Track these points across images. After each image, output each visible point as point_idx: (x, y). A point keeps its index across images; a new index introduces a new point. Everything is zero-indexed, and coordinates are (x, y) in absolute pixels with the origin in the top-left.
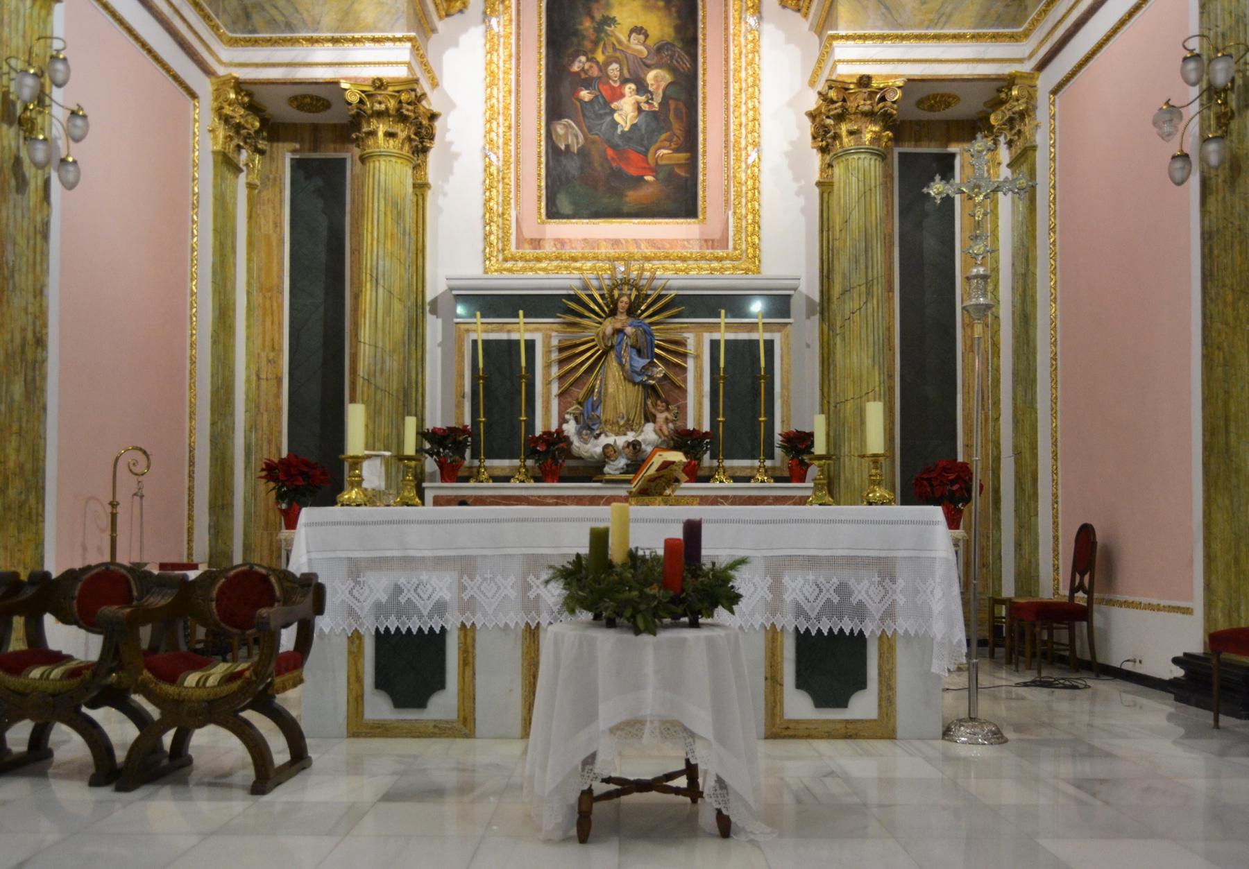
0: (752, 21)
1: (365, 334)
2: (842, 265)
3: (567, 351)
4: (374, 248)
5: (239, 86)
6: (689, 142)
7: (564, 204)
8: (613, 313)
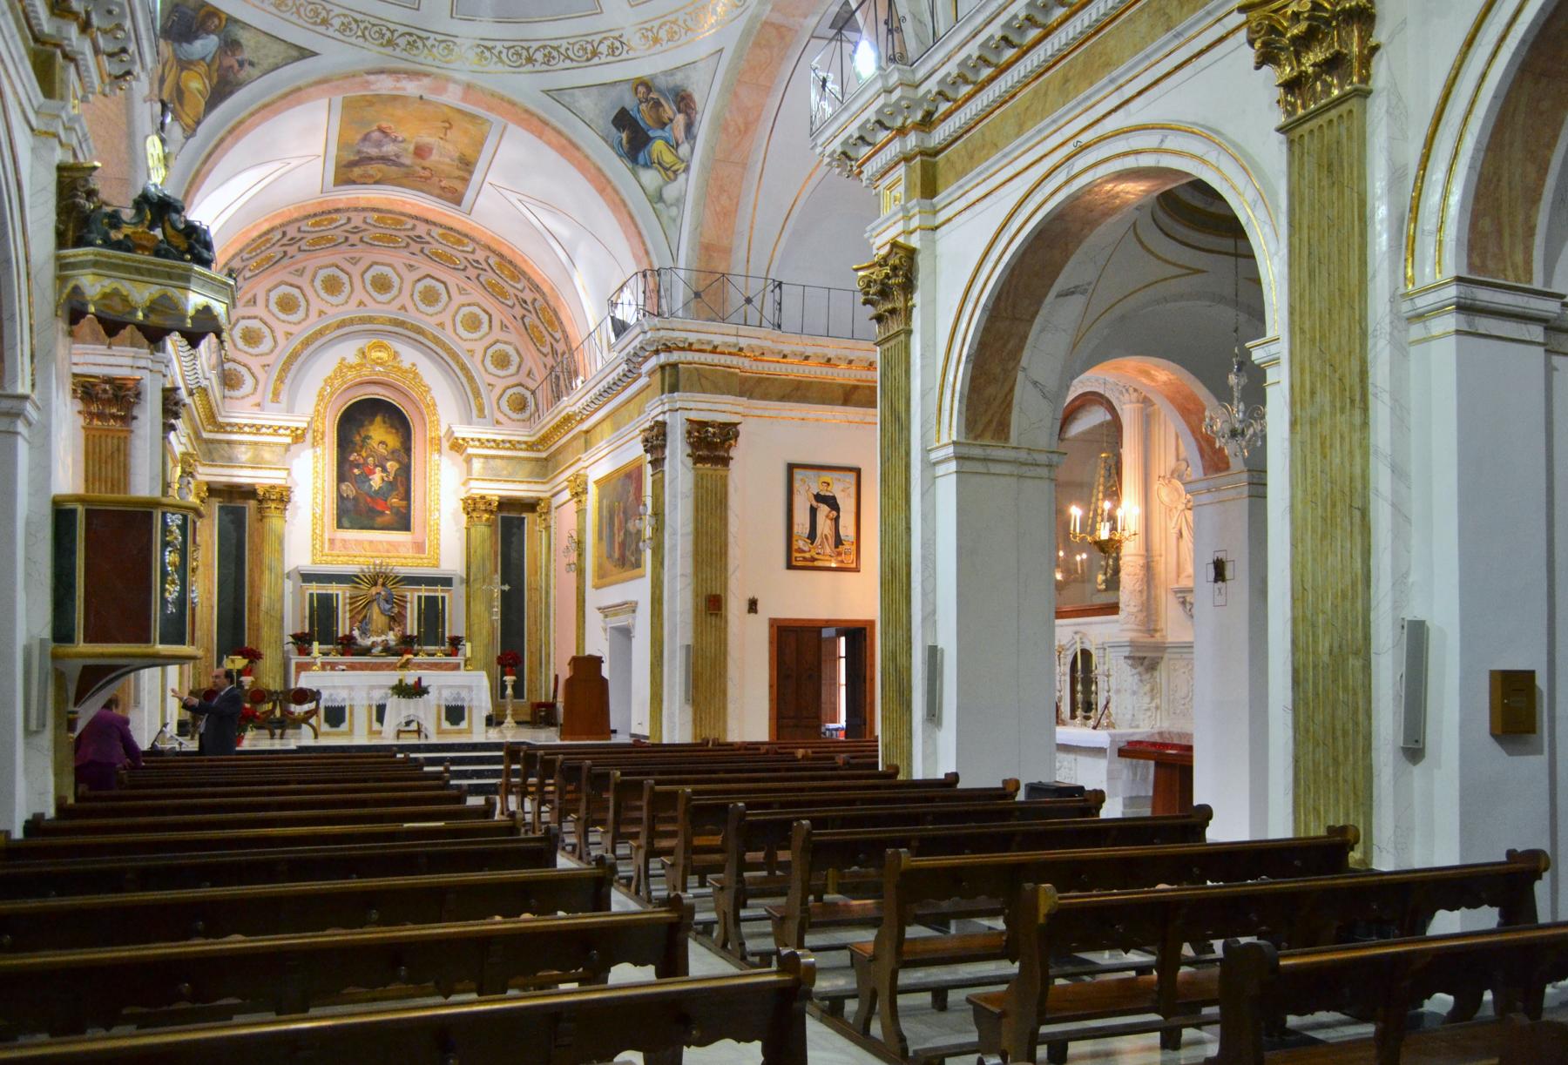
0: (436, 456)
1: (265, 593)
2: (473, 569)
3: (353, 599)
4: (268, 556)
5: (208, 484)
6: (407, 496)
7: (345, 522)
8: (375, 584)
